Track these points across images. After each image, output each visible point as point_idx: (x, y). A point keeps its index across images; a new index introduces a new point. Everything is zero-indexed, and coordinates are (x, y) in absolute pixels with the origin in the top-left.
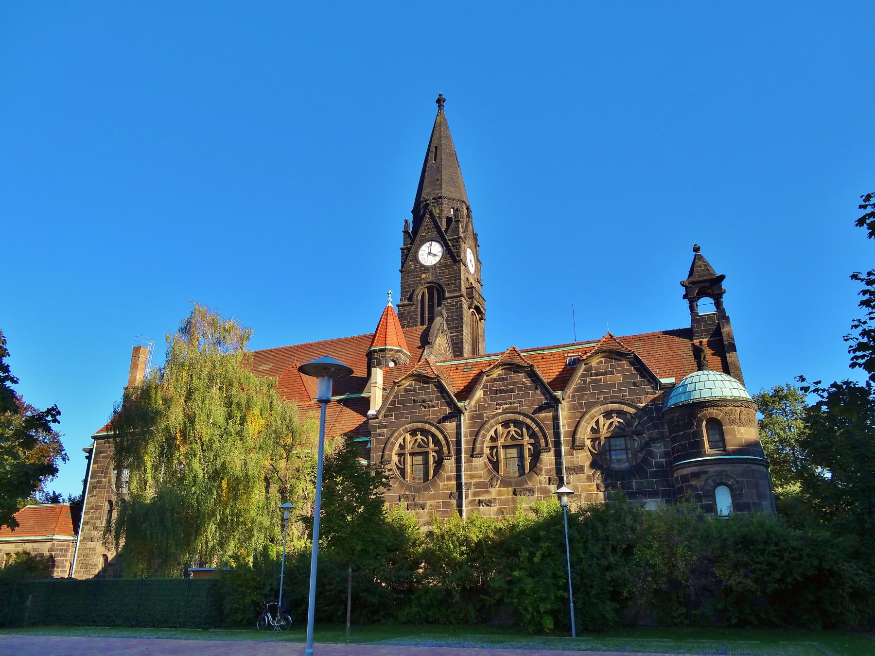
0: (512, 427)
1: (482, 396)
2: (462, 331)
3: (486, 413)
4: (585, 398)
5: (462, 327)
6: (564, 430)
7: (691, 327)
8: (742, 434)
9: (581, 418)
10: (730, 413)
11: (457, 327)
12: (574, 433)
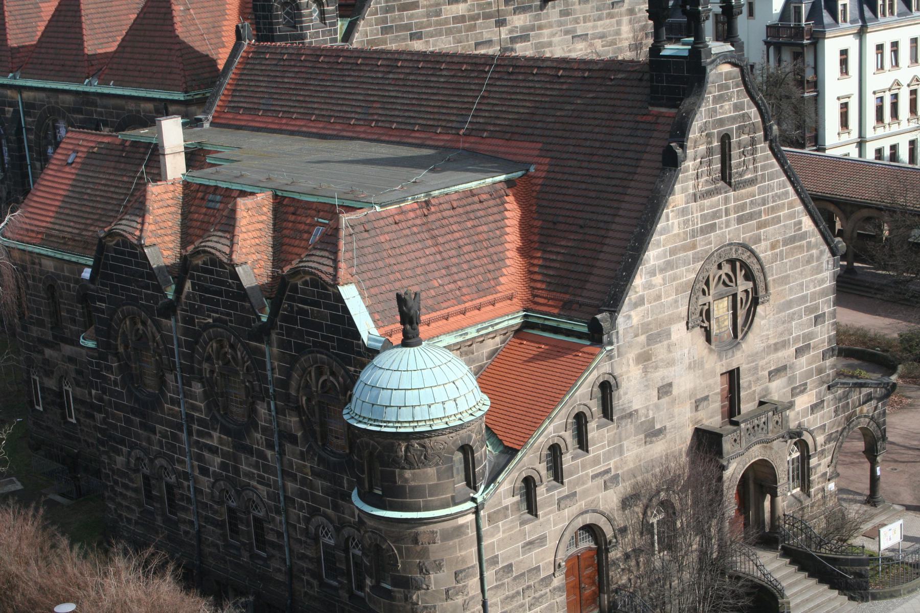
8: (406, 480)
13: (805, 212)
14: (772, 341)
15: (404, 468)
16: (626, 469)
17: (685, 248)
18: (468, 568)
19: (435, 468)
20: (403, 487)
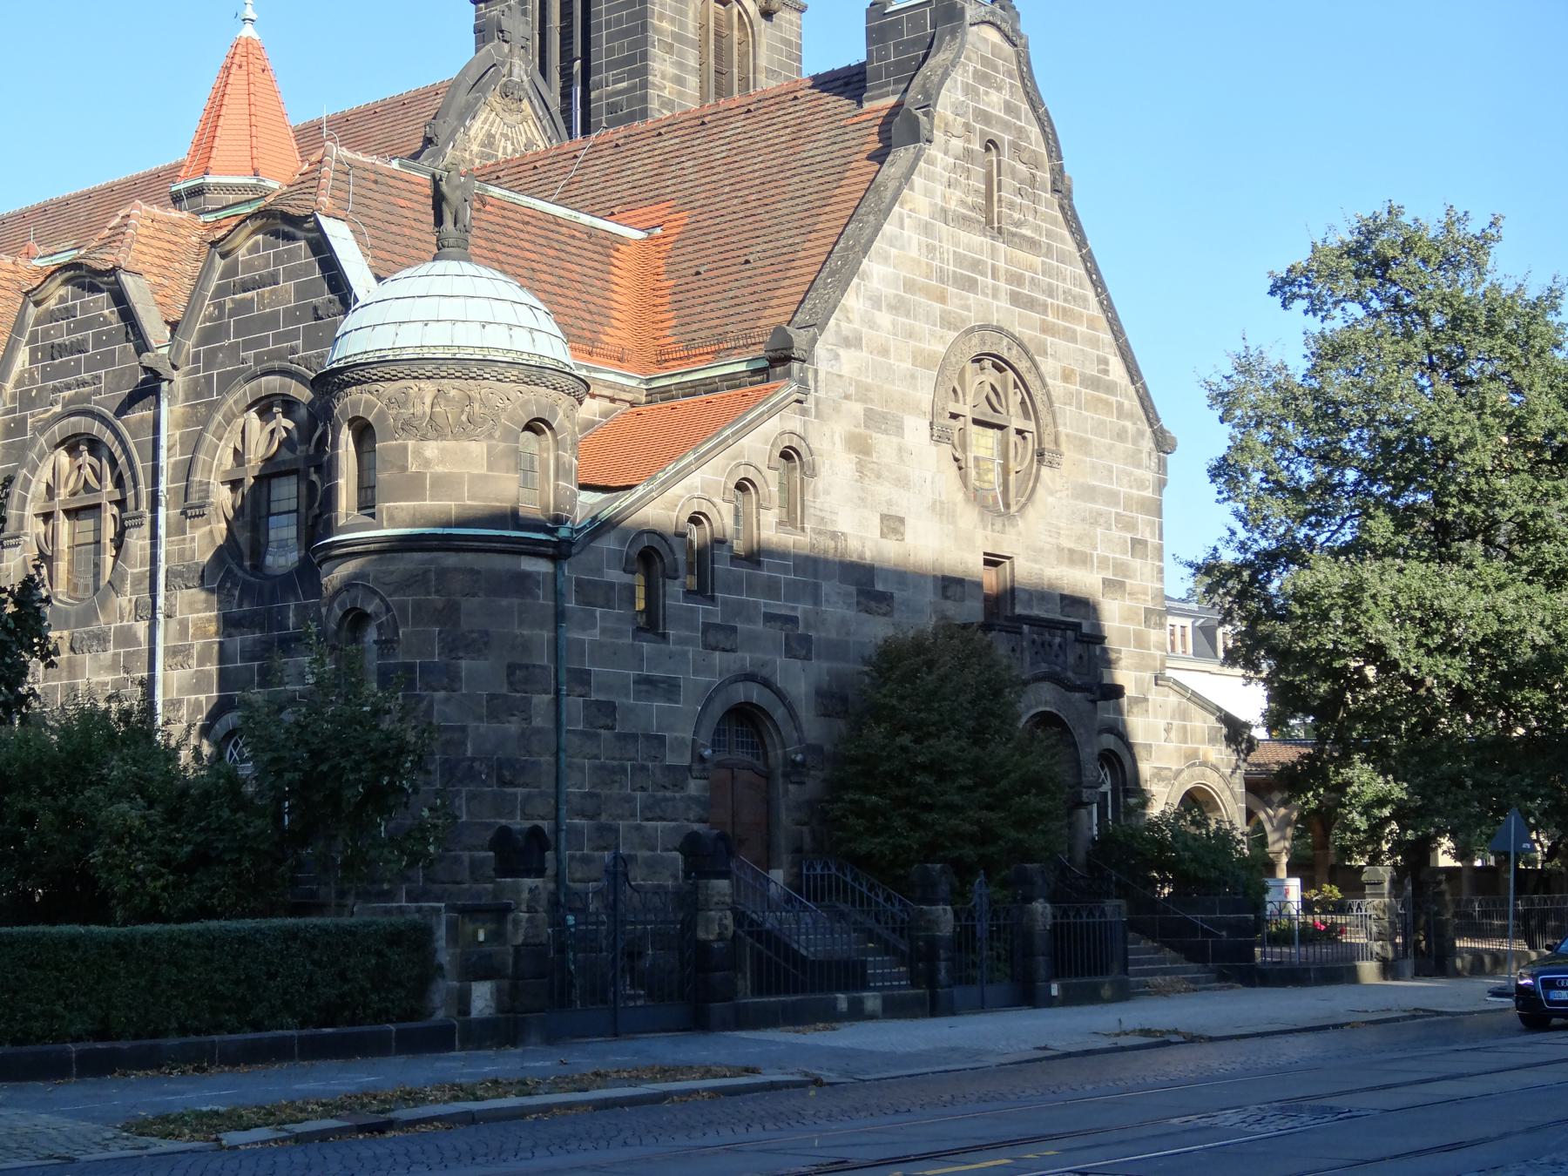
0: (86, 454)
1: (27, 366)
2: (644, 71)
3: (33, 416)
4: (219, 360)
5: (644, 56)
6: (172, 460)
7: (863, 58)
8: (427, 463)
9: (205, 423)
10: (402, 401)
11: (630, 60)
12: (188, 468)
13: (1114, 349)
14: (1068, 544)
15: (424, 438)
16: (823, 635)
17: (927, 291)
18: (534, 666)
19: (484, 445)
20: (420, 476)
